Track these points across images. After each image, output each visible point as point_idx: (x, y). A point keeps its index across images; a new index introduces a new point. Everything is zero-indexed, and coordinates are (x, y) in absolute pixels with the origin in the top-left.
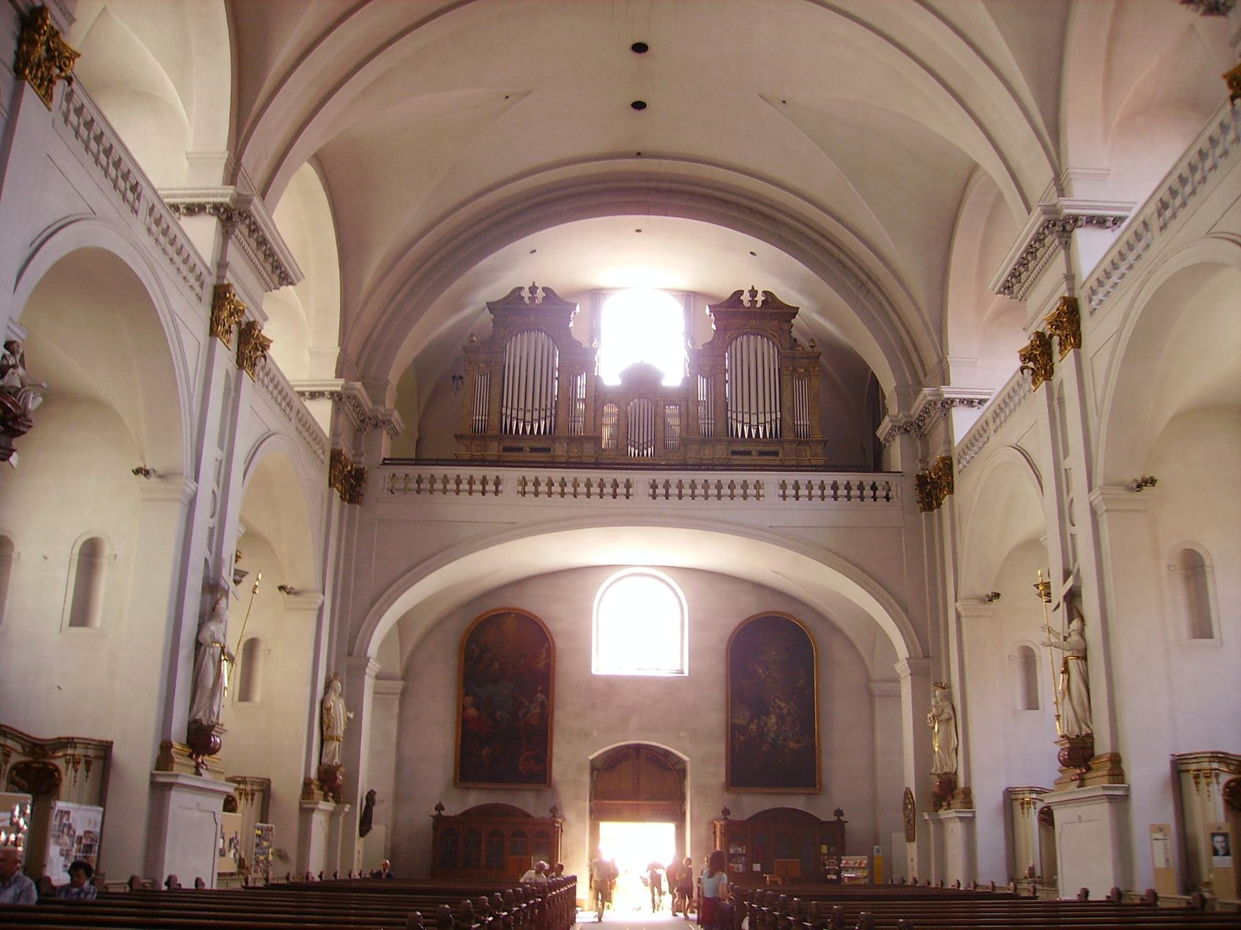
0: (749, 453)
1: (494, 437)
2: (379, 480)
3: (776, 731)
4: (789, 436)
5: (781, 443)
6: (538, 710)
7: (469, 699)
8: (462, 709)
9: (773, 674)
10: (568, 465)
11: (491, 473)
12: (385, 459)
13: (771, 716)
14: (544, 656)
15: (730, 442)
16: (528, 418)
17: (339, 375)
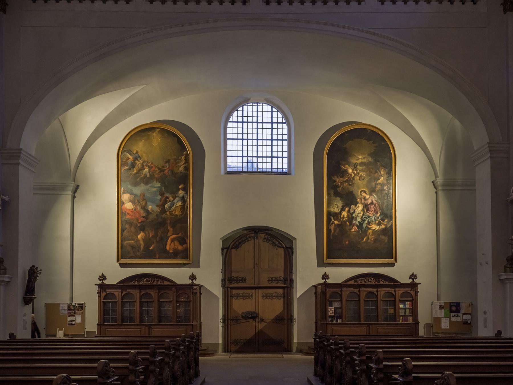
3: (362, 217)
9: (360, 174)
13: (358, 205)
14: (183, 162)
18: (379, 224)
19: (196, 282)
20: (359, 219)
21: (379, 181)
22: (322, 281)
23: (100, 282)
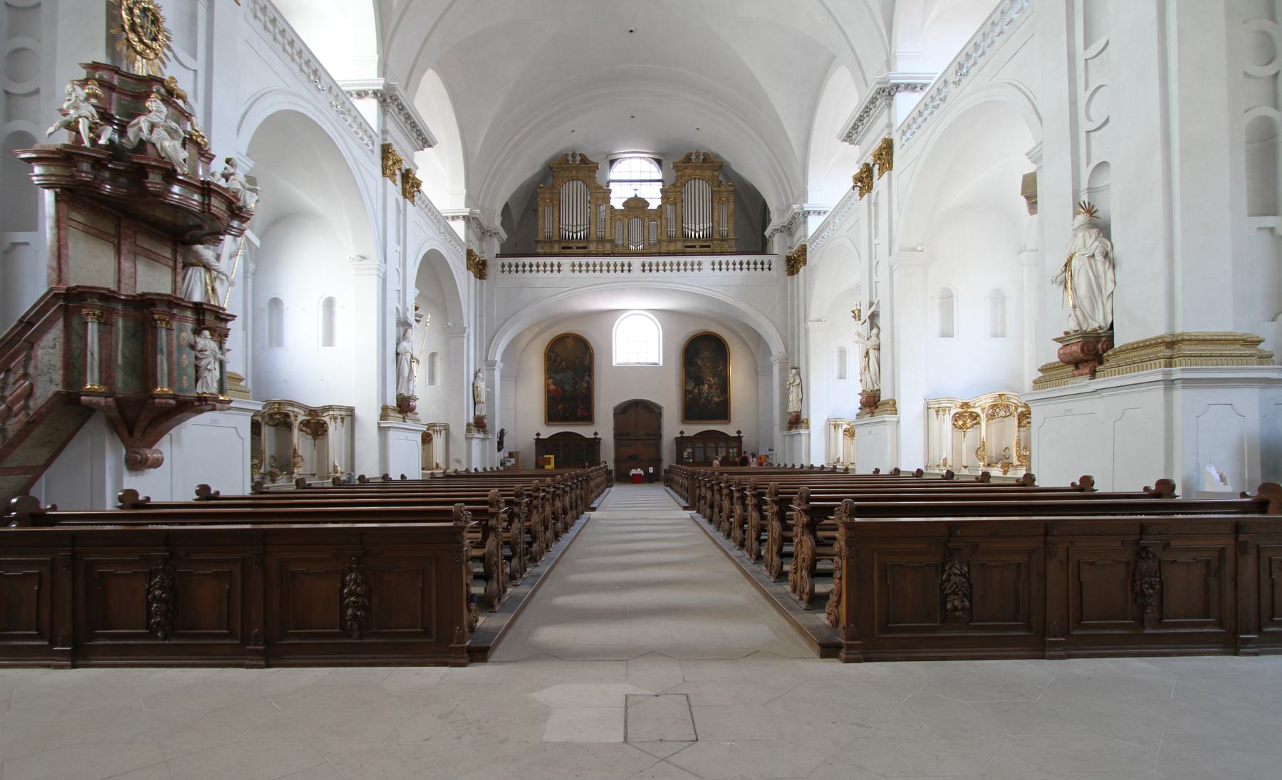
0: (694, 247)
1: (556, 242)
2: (495, 265)
4: (716, 236)
5: (712, 241)
6: (586, 385)
7: (551, 381)
8: (547, 386)
10: (597, 255)
11: (555, 260)
12: (497, 255)
15: (684, 241)
16: (575, 230)
17: (467, 206)
18: (719, 397)
19: (598, 437)
20: (705, 394)
21: (719, 369)
22: (680, 435)
23: (536, 437)
